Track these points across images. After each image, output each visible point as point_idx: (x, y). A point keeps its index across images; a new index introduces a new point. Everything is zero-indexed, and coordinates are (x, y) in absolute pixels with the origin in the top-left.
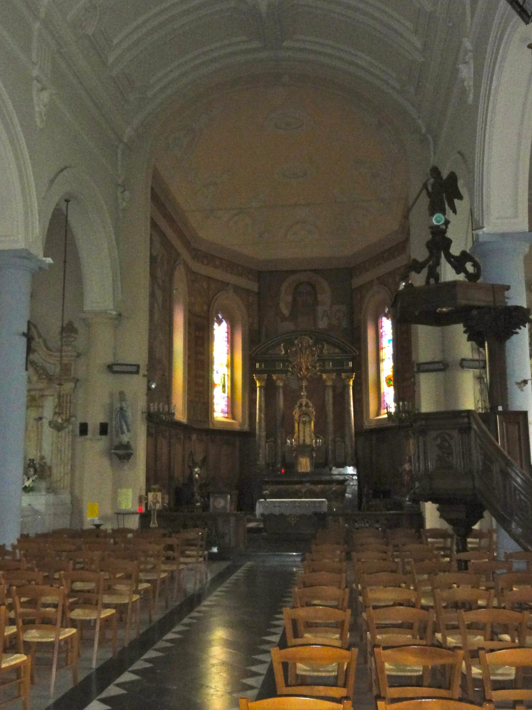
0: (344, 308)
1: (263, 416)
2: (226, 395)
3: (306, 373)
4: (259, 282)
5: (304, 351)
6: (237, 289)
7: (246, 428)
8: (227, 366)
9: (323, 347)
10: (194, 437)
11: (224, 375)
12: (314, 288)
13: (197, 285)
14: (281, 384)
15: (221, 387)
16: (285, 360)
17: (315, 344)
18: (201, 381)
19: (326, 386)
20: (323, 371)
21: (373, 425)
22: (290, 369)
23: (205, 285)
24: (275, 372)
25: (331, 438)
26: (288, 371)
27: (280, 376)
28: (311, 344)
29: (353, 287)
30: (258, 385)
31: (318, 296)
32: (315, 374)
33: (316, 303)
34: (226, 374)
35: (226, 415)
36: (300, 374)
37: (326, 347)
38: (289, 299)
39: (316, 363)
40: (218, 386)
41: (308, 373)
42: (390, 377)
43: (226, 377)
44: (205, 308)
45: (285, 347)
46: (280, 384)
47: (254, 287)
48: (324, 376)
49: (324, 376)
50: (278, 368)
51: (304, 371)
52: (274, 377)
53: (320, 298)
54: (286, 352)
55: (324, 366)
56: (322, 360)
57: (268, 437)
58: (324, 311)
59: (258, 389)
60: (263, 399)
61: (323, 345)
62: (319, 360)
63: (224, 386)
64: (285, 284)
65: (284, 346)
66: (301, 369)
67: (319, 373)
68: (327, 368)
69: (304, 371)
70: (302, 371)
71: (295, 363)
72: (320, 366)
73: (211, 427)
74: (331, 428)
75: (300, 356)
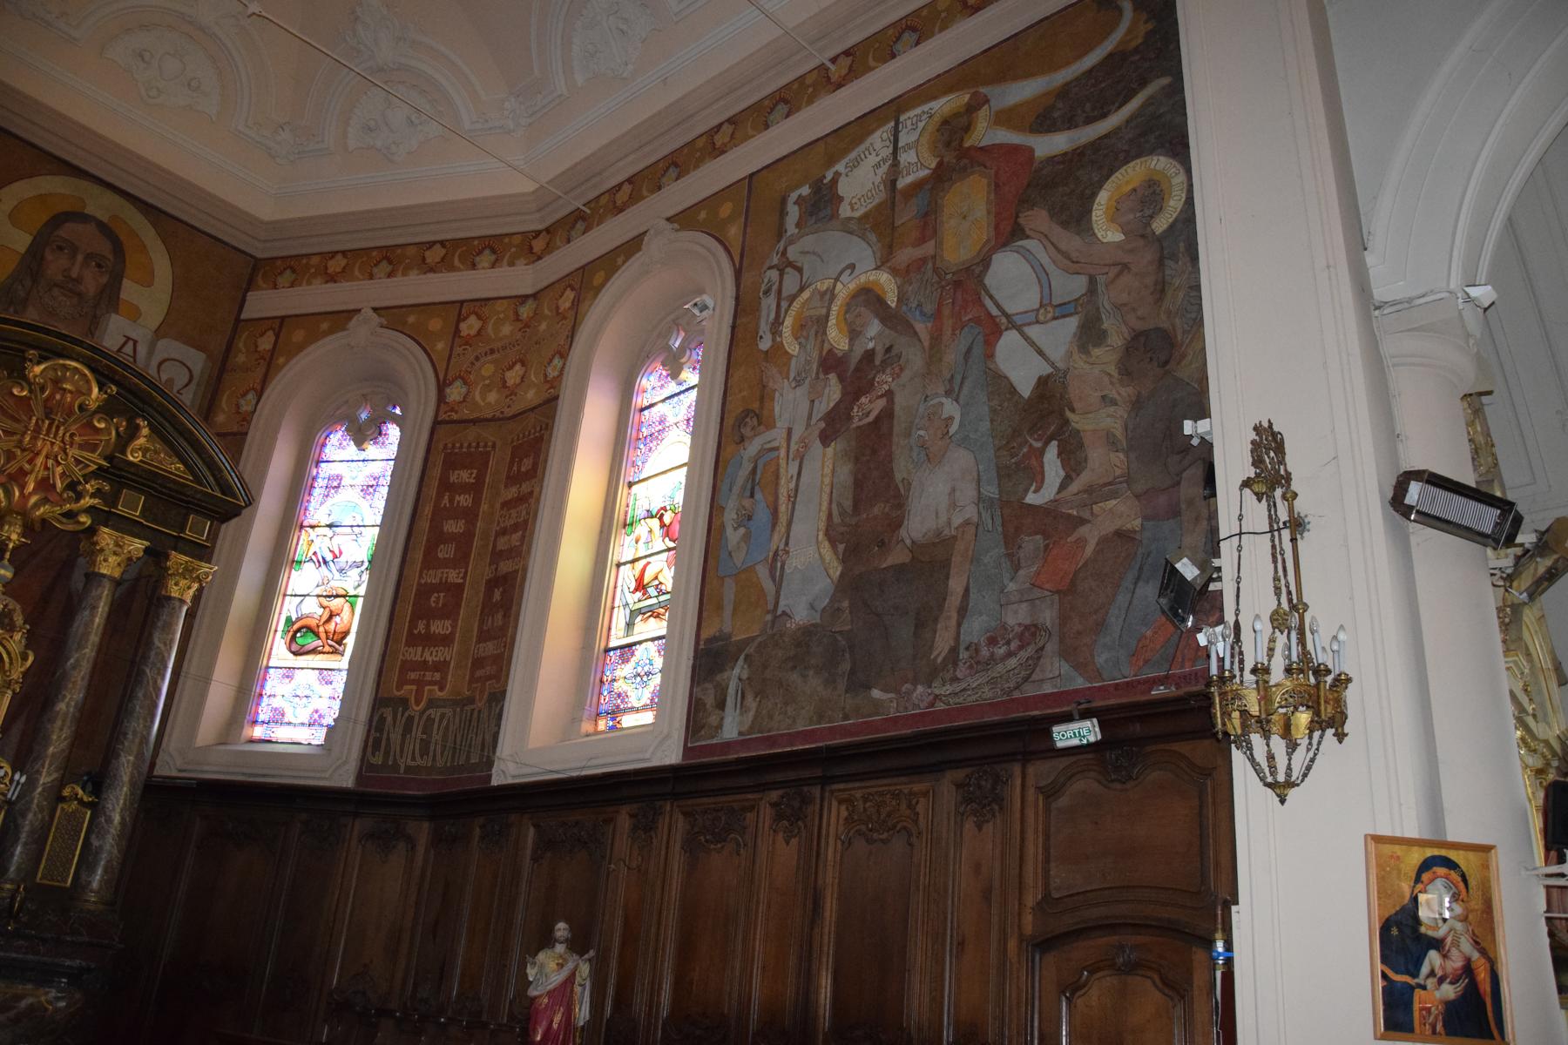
0: (197, 360)
3: (33, 500)
5: (58, 418)
9: (133, 432)
12: (118, 249)
17: (108, 409)
19: (93, 578)
20: (103, 517)
21: (214, 770)
25: (46, 778)
29: (243, 316)
31: (126, 283)
32: (70, 515)
33: (110, 297)
37: (141, 441)
39: (87, 478)
41: (45, 501)
42: (313, 623)
48: (106, 536)
49: (106, 536)
51: (31, 486)
53: (130, 290)
55: (111, 499)
56: (117, 473)
58: (128, 339)
61: (138, 428)
62: (100, 473)
67: (85, 519)
68: (121, 509)
69: (31, 486)
70: (22, 487)
72: (98, 493)
74: (58, 739)
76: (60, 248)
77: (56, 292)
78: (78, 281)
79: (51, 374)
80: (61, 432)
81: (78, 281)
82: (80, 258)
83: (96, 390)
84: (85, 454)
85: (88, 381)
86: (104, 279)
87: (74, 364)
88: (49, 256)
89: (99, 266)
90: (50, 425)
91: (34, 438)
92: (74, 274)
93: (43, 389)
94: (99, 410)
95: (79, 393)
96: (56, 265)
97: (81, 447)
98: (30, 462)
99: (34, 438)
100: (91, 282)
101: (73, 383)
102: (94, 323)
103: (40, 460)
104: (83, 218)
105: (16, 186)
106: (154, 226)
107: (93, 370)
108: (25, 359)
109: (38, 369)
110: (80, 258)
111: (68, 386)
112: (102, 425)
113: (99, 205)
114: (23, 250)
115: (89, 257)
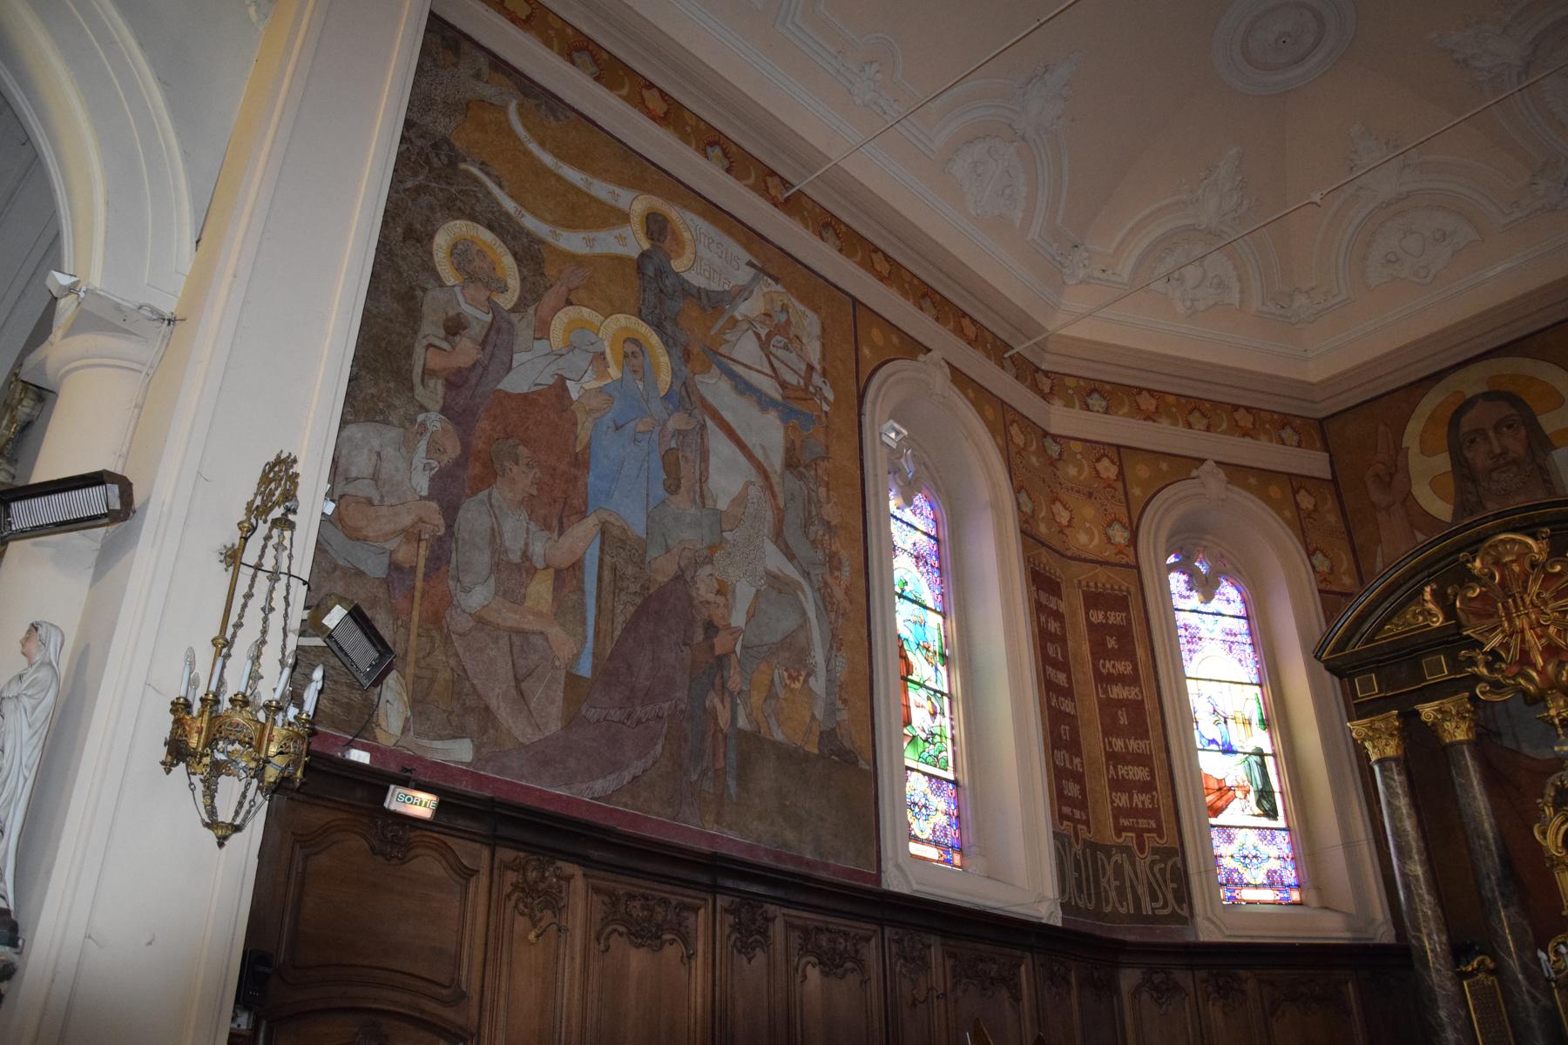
1: (1418, 870)
2: (1281, 822)
3: (1550, 668)
4: (1326, 449)
5: (1516, 590)
6: (1236, 473)
7: (1384, 934)
8: (1266, 723)
10: (1129, 979)
11: (1260, 753)
12: (1513, 399)
13: (1072, 471)
14: (1461, 735)
15: (1252, 797)
16: (1452, 641)
18: (1138, 773)
22: (1485, 671)
23: (1108, 469)
24: (1429, 694)
26: (1477, 678)
27: (1449, 704)
28: (1542, 558)
30: (1373, 758)
31: (1542, 419)
34: (1267, 749)
35: (1295, 896)
36: (1530, 679)
38: (1443, 462)
40: (1239, 794)
43: (1269, 761)
44: (1120, 535)
45: (1439, 597)
46: (1458, 732)
47: (1315, 463)
50: (1431, 679)
51: (1540, 661)
52: (1428, 711)
54: (1449, 612)
57: (1459, 952)
59: (1377, 769)
60: (1403, 803)
63: (1265, 794)
64: (1414, 428)
65: (1433, 592)
66: (1525, 659)
69: (1540, 661)
70: (1533, 666)
71: (1494, 642)
73: (1207, 933)
75: (1506, 608)
76: (1473, 441)
77: (1495, 475)
78: (1505, 452)
79: (1489, 559)
80: (1528, 601)
81: (1505, 452)
82: (1491, 434)
83: (1530, 541)
84: (1560, 603)
85: (1521, 542)
86: (1523, 432)
87: (1502, 537)
88: (1469, 455)
89: (1509, 427)
90: (1514, 601)
91: (1510, 620)
92: (1498, 451)
93: (1492, 577)
94: (1550, 555)
95: (1520, 558)
96: (1479, 457)
97: (1556, 598)
98: (1523, 641)
99: (1510, 620)
100: (1516, 447)
101: (1508, 553)
102: (1544, 475)
103: (1529, 635)
104: (1469, 403)
105: (1409, 428)
106: (1525, 355)
107: (1514, 530)
108: (1463, 564)
109: (1478, 563)
110: (1491, 434)
111: (1507, 559)
112: (1558, 568)
113: (1471, 383)
114: (1449, 468)
115: (1496, 428)
